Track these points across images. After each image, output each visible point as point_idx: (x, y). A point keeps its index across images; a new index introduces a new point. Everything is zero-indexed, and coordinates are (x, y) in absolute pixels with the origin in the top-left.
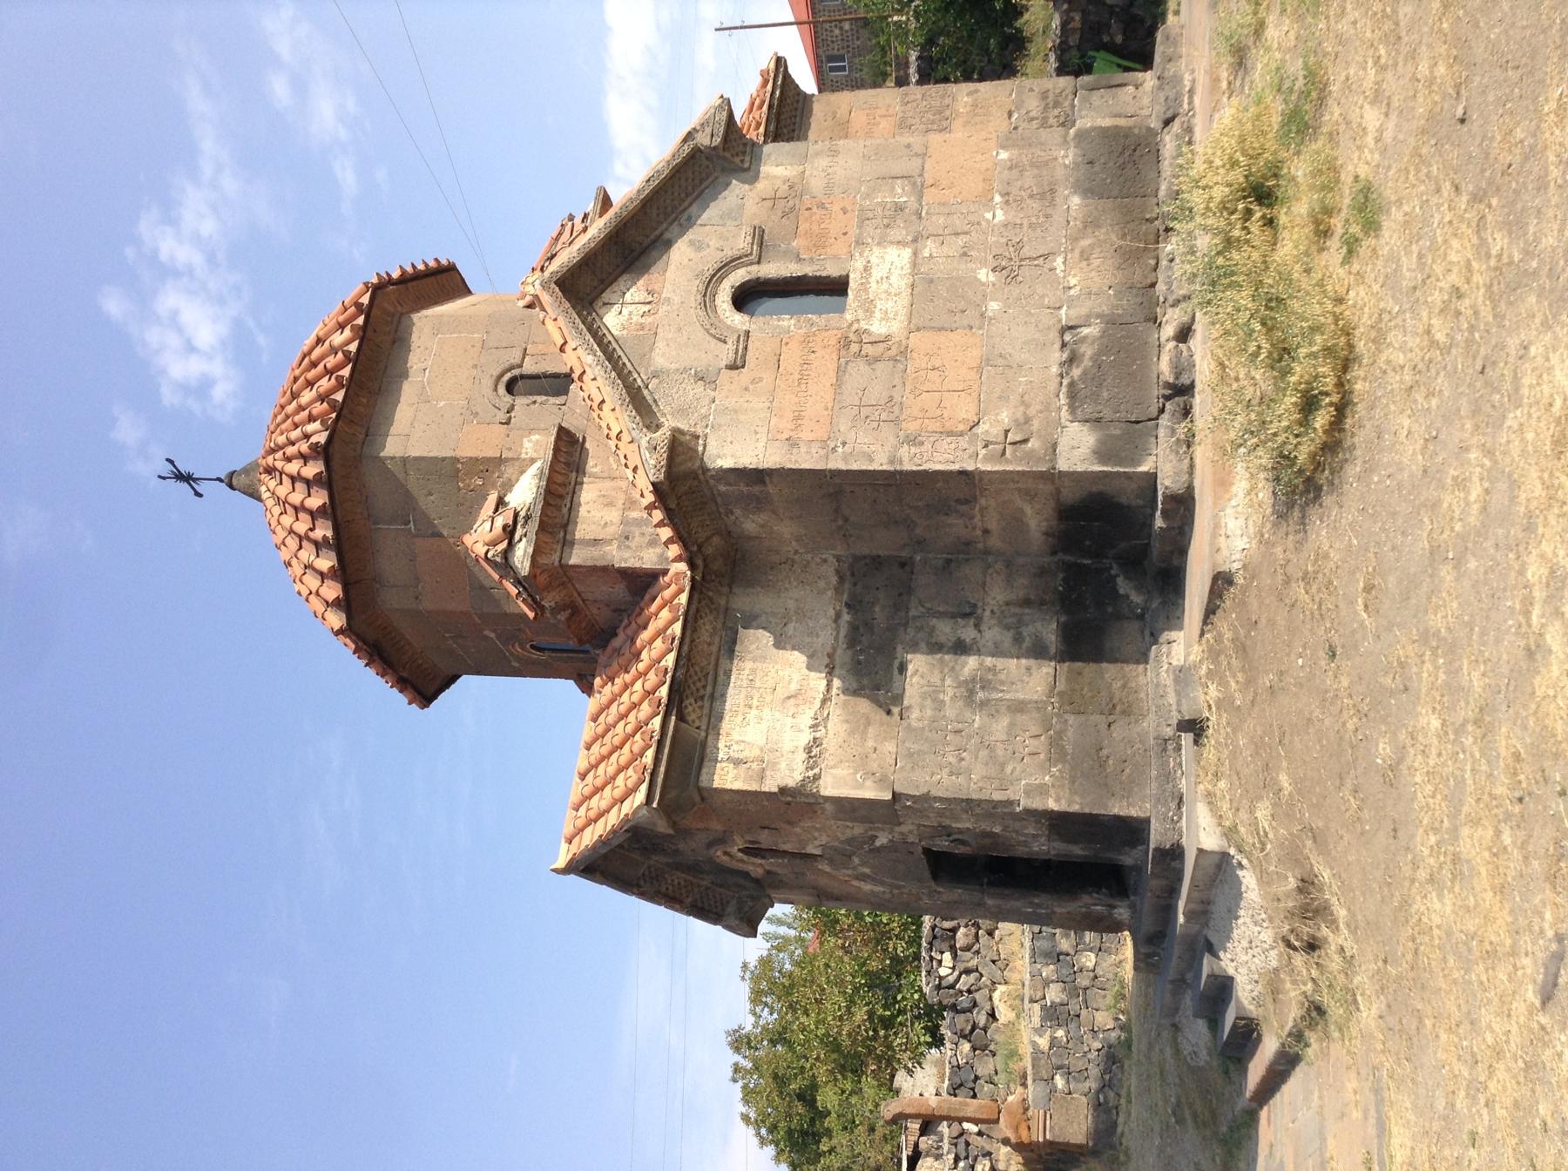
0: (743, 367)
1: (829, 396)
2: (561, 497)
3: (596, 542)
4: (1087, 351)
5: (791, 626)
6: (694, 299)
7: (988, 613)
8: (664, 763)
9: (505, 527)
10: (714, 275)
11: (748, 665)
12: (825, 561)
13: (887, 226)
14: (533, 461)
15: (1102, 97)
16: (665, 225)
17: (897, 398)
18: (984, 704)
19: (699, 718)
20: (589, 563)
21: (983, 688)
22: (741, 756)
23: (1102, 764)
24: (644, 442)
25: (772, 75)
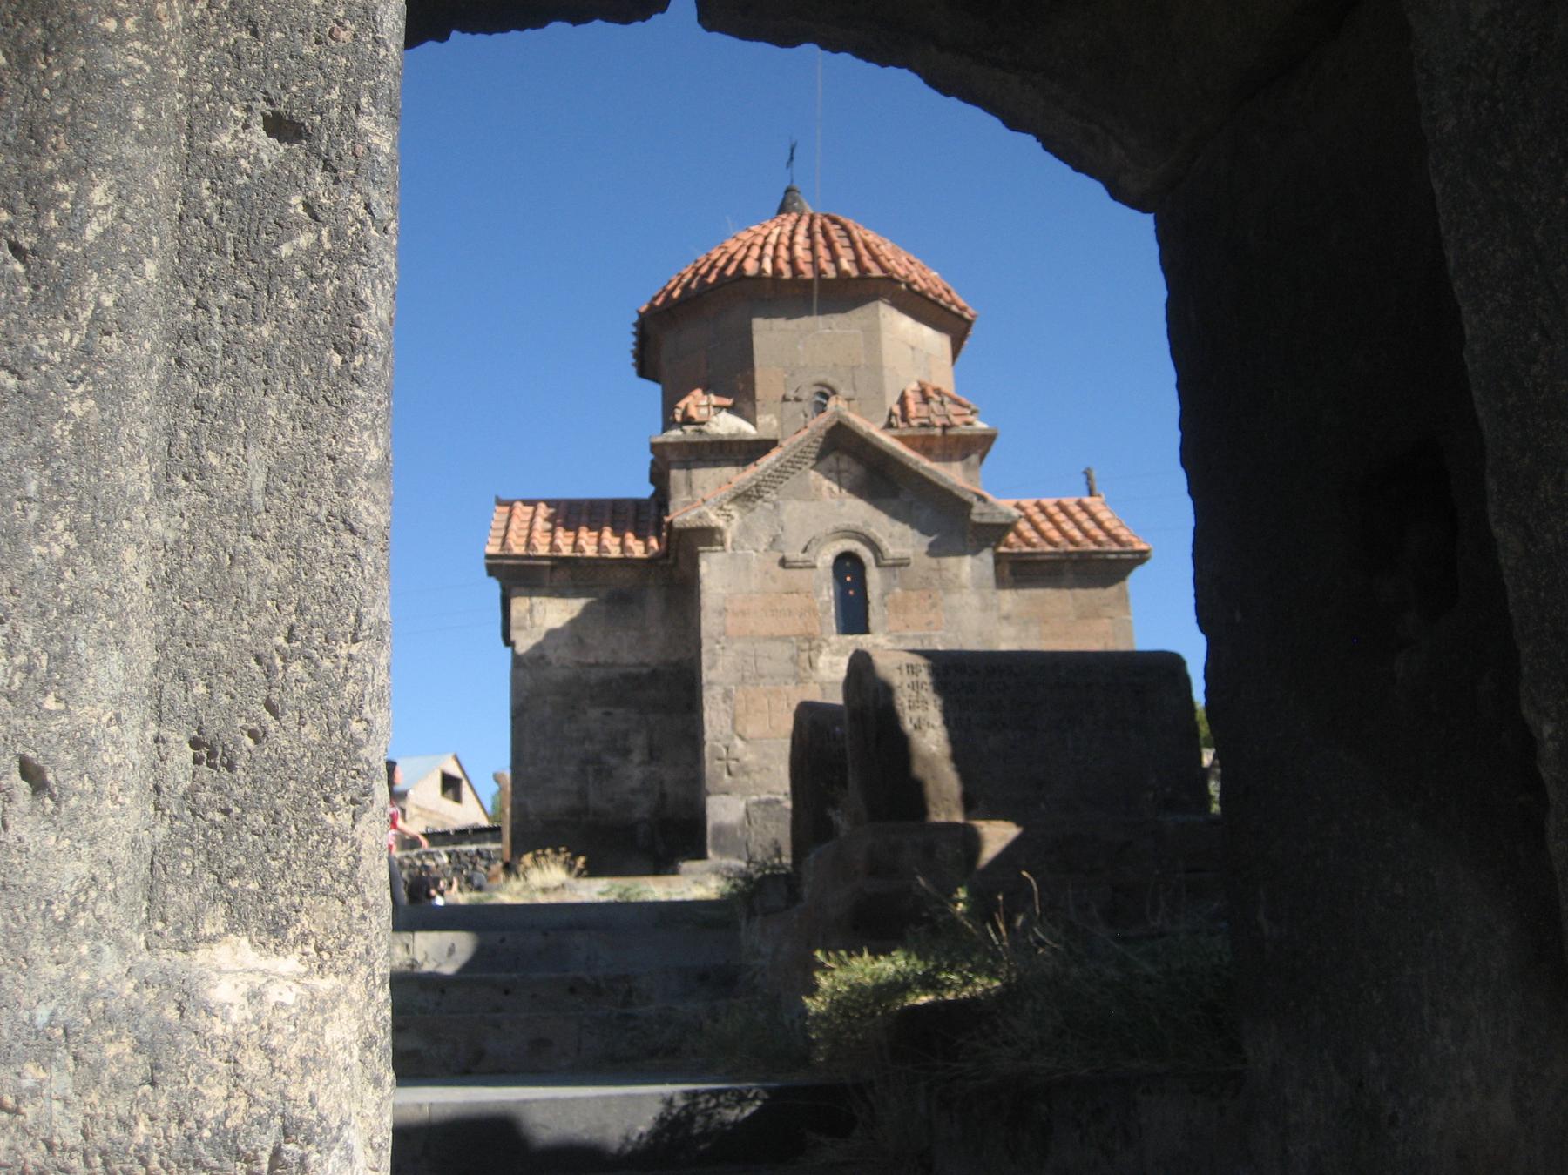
3: (689, 484)
6: (844, 523)
7: (653, 769)
9: (693, 418)
10: (863, 534)
14: (754, 424)
22: (535, 613)
24: (704, 508)
25: (1129, 548)
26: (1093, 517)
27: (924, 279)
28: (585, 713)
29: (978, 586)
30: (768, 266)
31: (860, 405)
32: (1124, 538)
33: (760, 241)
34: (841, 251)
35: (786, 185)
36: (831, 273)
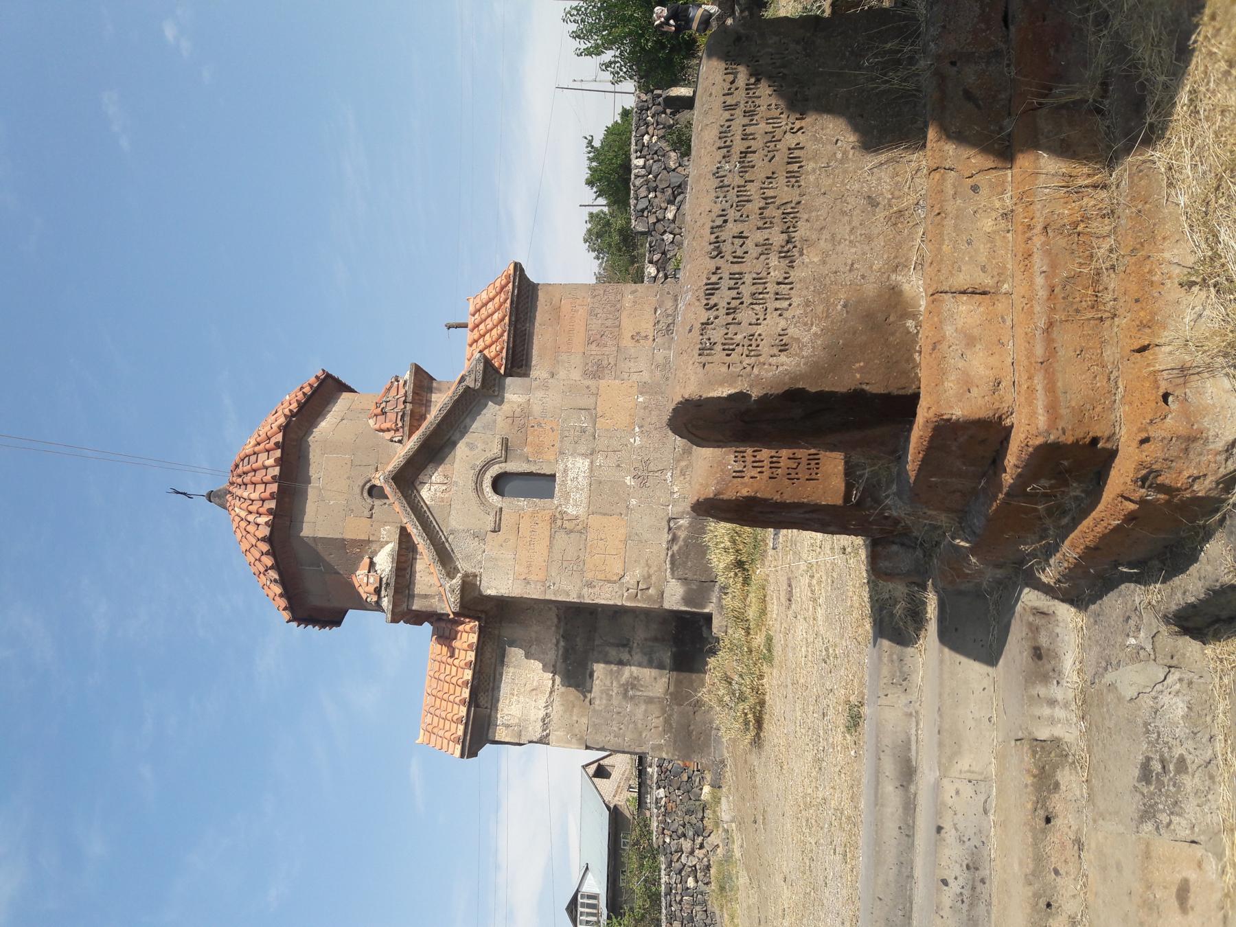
1: (546, 553)
2: (405, 569)
3: (426, 596)
4: (682, 535)
6: (471, 485)
7: (635, 645)
8: (469, 735)
11: (511, 670)
12: (550, 609)
13: (576, 443)
14: (387, 543)
16: (451, 432)
17: (582, 557)
18: (632, 698)
20: (424, 609)
21: (632, 689)
23: (690, 734)
25: (512, 278)
29: (529, 390)
31: (381, 463)
32: (503, 283)
34: (259, 464)
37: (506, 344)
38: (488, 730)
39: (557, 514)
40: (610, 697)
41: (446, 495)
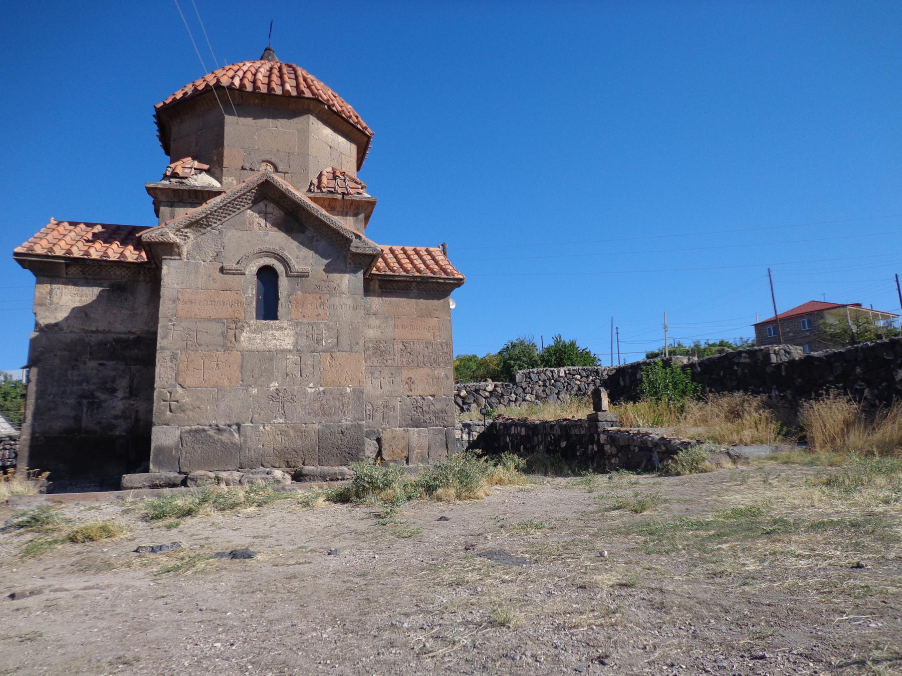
0: (223, 274)
2: (196, 198)
3: (173, 216)
4: (224, 437)
5: (128, 312)
6: (265, 247)
7: (132, 402)
10: (278, 255)
14: (221, 183)
15: (441, 440)
18: (80, 404)
19: (72, 273)
21: (89, 402)
22: (53, 295)
24: (166, 229)
25: (451, 277)
26: (433, 258)
27: (342, 107)
28: (85, 363)
29: (352, 293)
30: (237, 82)
32: (449, 271)
33: (236, 68)
35: (267, 46)
36: (278, 91)
37: (397, 274)
38: (47, 276)
39: (241, 324)
40: (80, 383)
41: (255, 227)
